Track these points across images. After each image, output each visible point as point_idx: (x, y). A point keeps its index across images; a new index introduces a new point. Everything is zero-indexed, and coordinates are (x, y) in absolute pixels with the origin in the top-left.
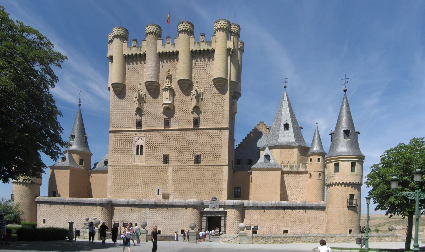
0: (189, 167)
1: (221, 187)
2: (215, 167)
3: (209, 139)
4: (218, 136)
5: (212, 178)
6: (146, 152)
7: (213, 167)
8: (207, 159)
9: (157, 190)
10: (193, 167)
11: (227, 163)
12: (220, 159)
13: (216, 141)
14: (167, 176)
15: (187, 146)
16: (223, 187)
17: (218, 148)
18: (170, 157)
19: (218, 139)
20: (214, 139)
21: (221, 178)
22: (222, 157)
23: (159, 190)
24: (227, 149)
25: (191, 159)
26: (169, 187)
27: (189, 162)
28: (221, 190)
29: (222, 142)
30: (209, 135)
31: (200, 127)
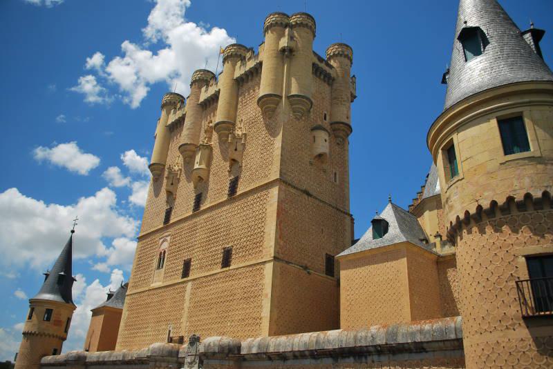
0: (213, 278)
2: (251, 269)
4: (261, 202)
7: (248, 269)
9: (168, 332)
10: (218, 276)
11: (273, 255)
12: (261, 248)
14: (183, 300)
16: (262, 315)
19: (261, 207)
21: (260, 293)
23: (170, 331)
25: (218, 261)
26: (182, 325)
29: (268, 211)
31: (238, 193)
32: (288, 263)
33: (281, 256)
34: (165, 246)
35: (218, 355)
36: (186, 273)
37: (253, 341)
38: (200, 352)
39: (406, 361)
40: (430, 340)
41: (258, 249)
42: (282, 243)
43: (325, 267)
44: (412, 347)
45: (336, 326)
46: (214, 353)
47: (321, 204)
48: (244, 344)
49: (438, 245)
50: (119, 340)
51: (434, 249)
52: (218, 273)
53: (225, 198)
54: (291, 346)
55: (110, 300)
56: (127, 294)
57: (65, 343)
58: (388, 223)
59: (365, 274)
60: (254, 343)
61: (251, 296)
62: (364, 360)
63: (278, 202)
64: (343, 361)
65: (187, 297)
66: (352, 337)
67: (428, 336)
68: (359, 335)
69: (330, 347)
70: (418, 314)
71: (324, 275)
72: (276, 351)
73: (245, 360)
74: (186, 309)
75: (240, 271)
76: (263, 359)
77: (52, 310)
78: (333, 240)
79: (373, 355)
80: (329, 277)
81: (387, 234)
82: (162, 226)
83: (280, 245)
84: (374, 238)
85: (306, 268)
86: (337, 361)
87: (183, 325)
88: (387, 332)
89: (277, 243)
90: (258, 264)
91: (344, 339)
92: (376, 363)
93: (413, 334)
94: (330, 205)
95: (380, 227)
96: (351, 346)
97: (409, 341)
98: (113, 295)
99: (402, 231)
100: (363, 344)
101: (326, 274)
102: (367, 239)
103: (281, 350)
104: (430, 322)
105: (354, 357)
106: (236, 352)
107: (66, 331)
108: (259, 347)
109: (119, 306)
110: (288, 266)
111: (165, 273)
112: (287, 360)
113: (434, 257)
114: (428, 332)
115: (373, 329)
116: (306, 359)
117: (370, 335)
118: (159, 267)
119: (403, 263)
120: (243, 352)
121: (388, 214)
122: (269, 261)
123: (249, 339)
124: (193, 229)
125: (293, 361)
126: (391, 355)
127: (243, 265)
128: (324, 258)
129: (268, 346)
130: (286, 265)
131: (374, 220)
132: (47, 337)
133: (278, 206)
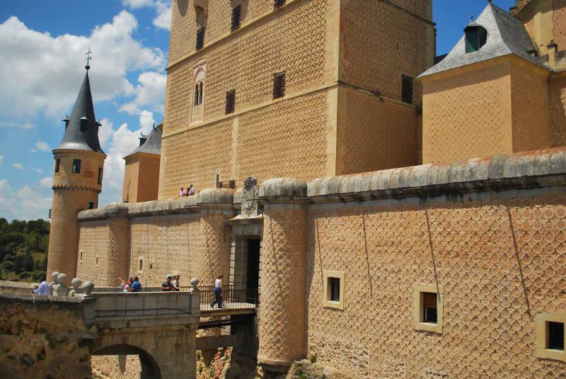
1: (322, 152)
2: (310, 98)
3: (302, 26)
4: (319, 12)
5: (305, 130)
6: (206, 95)
7: (306, 98)
8: (296, 80)
11: (337, 80)
13: (314, 26)
15: (263, 60)
16: (327, 152)
17: (318, 43)
18: (236, 95)
19: (319, 18)
20: (310, 22)
22: (326, 65)
23: (218, 176)
24: (337, 39)
27: (265, 98)
28: (321, 159)
30: (302, 15)
32: (355, 88)
33: (347, 80)
34: (201, 76)
35: (281, 198)
36: (230, 108)
37: (321, 181)
38: (260, 195)
39: (513, 198)
40: (546, 173)
41: (317, 73)
42: (347, 63)
43: (401, 92)
44: (522, 182)
45: (417, 160)
46: (276, 197)
47: (396, 11)
48: (311, 185)
49: (552, 58)
50: (160, 189)
51: (546, 64)
52: (270, 105)
53: (271, 10)
54: (367, 185)
55: (144, 145)
56: (162, 136)
57: (100, 195)
58: (486, 31)
59: (455, 99)
60: (322, 183)
61: (312, 131)
62: (459, 198)
63: (341, 10)
64: (432, 200)
65: (235, 135)
66: (445, 172)
67: (543, 169)
68: (454, 169)
69: (417, 185)
70: (521, 143)
71: (401, 102)
72: (350, 191)
73: (312, 203)
74: (234, 150)
75: (297, 101)
76: (335, 202)
77: (80, 160)
78: (411, 58)
79: (470, 192)
80: (406, 104)
81: (485, 45)
82: (194, 52)
83: (345, 66)
84: (467, 51)
85: (377, 94)
86: (425, 201)
87: (233, 168)
88: (490, 166)
89: (341, 63)
90: (319, 91)
91: (435, 175)
92: (474, 202)
93: (524, 167)
94: (407, 12)
95: (476, 36)
96: (443, 183)
97: (519, 175)
98: (146, 139)
99: (505, 40)
100: (459, 179)
101: (403, 100)
102: (458, 54)
103: (357, 190)
104: (547, 152)
105: (447, 195)
106: (302, 194)
107: (100, 183)
108: (329, 187)
109: (154, 151)
110: (357, 93)
111: (205, 109)
112: (363, 201)
113: (545, 74)
114: (544, 164)
115: (472, 163)
116: (386, 199)
117: (468, 169)
118: (196, 103)
119: (505, 83)
120: (310, 194)
121: (486, 19)
122: (332, 87)
123: (317, 180)
124: (234, 53)
125: (370, 202)
126: (494, 192)
127: (297, 94)
128: (400, 80)
129: (340, 186)
130: (353, 91)
131: (468, 27)
132: (80, 190)
133: (341, 16)
